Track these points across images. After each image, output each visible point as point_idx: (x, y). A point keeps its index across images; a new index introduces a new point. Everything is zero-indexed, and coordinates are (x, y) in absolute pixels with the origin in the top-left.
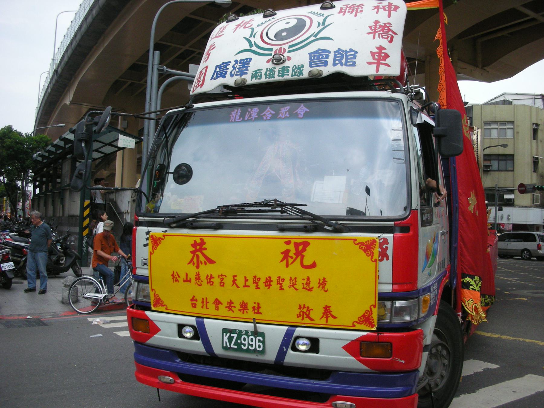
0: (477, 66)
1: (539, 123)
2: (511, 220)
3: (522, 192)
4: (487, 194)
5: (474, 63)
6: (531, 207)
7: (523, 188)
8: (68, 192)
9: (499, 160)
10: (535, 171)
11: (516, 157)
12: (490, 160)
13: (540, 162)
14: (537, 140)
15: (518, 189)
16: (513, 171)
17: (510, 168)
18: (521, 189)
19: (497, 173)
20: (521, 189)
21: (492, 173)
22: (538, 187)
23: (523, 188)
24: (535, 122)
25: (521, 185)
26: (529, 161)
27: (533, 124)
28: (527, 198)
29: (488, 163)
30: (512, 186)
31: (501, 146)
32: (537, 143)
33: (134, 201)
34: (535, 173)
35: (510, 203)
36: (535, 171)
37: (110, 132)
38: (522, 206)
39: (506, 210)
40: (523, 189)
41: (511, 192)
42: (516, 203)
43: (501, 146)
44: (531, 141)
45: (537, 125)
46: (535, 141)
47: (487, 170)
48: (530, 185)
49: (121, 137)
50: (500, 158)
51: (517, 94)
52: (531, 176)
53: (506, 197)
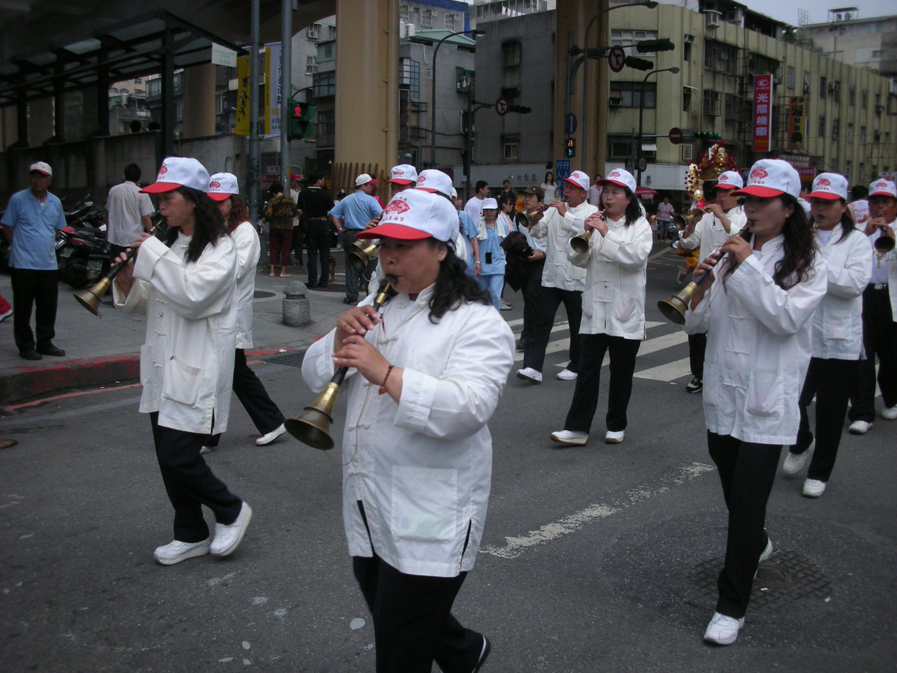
1: (693, 34)
2: (652, 184)
3: (675, 141)
4: (615, 144)
6: (680, 164)
7: (678, 136)
8: (101, 148)
9: (633, 91)
10: (685, 109)
11: (659, 87)
12: (620, 91)
13: (693, 95)
14: (690, 62)
15: (670, 136)
16: (654, 107)
17: (650, 104)
18: (673, 136)
19: (630, 110)
20: (673, 136)
21: (623, 110)
22: (702, 134)
23: (678, 136)
24: (687, 32)
25: (675, 131)
26: (676, 93)
27: (686, 36)
28: (674, 151)
29: (616, 95)
30: (652, 131)
31: (670, 70)
32: (689, 66)
33: (237, 156)
34: (685, 114)
35: (651, 158)
36: (685, 109)
37: (199, 37)
38: (668, 163)
39: (650, 169)
40: (676, 136)
41: (653, 140)
42: (658, 158)
43: (670, 70)
44: (681, 62)
45: (691, 38)
46: (686, 63)
47: (615, 104)
48: (688, 131)
49: (216, 46)
50: (635, 87)
52: (681, 116)
53: (645, 148)
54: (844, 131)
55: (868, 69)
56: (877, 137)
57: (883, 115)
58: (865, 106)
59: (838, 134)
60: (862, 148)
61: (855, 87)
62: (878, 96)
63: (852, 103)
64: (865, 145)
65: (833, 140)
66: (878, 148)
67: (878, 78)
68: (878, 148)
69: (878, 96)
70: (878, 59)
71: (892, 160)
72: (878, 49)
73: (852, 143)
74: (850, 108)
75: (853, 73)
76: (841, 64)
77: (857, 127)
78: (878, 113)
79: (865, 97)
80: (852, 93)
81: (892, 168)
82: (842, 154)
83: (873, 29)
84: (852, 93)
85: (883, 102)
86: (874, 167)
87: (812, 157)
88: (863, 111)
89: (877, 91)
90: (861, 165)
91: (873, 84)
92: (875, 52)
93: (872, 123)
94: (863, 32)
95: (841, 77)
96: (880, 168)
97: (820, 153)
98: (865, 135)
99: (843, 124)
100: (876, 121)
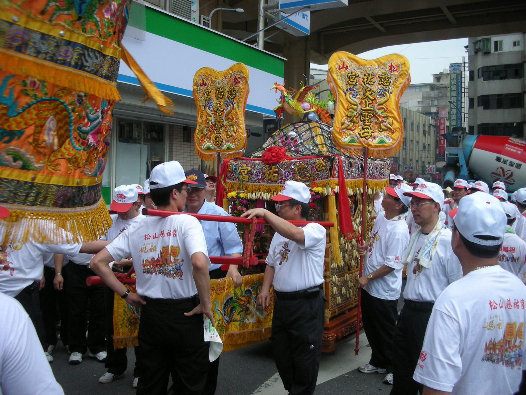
0: (321, 54)
5: (318, 51)
51: (316, 69)
54: (408, 144)
55: (419, 112)
56: (424, 147)
57: (426, 135)
58: (418, 131)
59: (406, 145)
60: (417, 152)
61: (413, 121)
62: (424, 125)
63: (412, 130)
64: (418, 151)
65: (404, 149)
66: (425, 152)
67: (424, 116)
68: (425, 152)
69: (424, 125)
70: (420, 105)
71: (432, 159)
72: (421, 100)
73: (412, 150)
74: (411, 132)
75: (412, 115)
76: (406, 109)
77: (415, 142)
78: (425, 135)
79: (418, 126)
80: (412, 124)
81: (432, 163)
82: (408, 156)
83: (417, 90)
84: (412, 124)
85: (427, 129)
86: (423, 162)
87: (394, 158)
88: (417, 134)
89: (423, 123)
90: (417, 161)
91: (422, 119)
92: (419, 102)
93: (422, 140)
94: (413, 91)
95: (406, 116)
96: (426, 163)
97: (397, 156)
98: (418, 145)
99: (408, 140)
100: (424, 137)
